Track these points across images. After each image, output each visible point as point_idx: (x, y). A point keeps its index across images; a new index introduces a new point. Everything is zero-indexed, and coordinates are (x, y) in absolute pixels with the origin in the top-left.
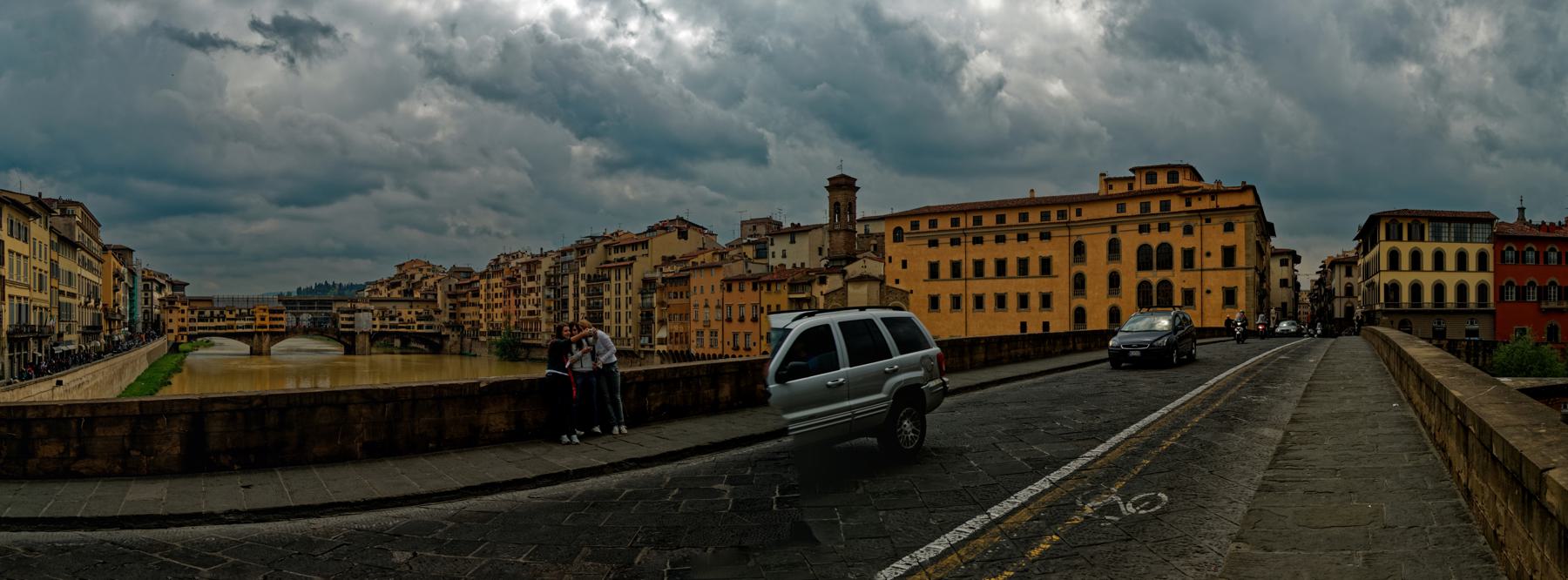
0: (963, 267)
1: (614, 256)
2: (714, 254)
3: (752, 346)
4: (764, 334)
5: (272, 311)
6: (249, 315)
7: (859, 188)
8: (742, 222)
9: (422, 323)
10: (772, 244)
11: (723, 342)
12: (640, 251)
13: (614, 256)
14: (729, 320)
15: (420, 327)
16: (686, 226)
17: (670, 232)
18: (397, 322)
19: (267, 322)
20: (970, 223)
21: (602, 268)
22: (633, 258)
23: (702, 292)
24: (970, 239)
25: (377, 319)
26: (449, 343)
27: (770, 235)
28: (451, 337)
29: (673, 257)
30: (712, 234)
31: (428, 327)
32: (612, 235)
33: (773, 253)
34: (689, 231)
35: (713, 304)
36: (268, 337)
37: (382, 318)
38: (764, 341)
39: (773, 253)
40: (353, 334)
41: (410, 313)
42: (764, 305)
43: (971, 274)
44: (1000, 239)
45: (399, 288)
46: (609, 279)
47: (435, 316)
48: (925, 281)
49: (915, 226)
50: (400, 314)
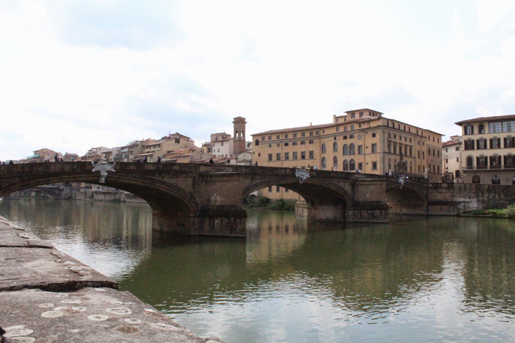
0: (281, 155)
1: (146, 150)
2: (190, 150)
7: (247, 122)
8: (211, 135)
10: (214, 146)
12: (157, 148)
13: (146, 150)
16: (179, 137)
17: (171, 140)
20: (284, 138)
22: (154, 152)
24: (284, 144)
26: (63, 193)
27: (213, 142)
28: (65, 190)
29: (172, 151)
30: (192, 141)
32: (146, 140)
33: (214, 150)
34: (181, 140)
39: (214, 150)
43: (284, 159)
44: (294, 144)
48: (267, 162)
49: (263, 139)
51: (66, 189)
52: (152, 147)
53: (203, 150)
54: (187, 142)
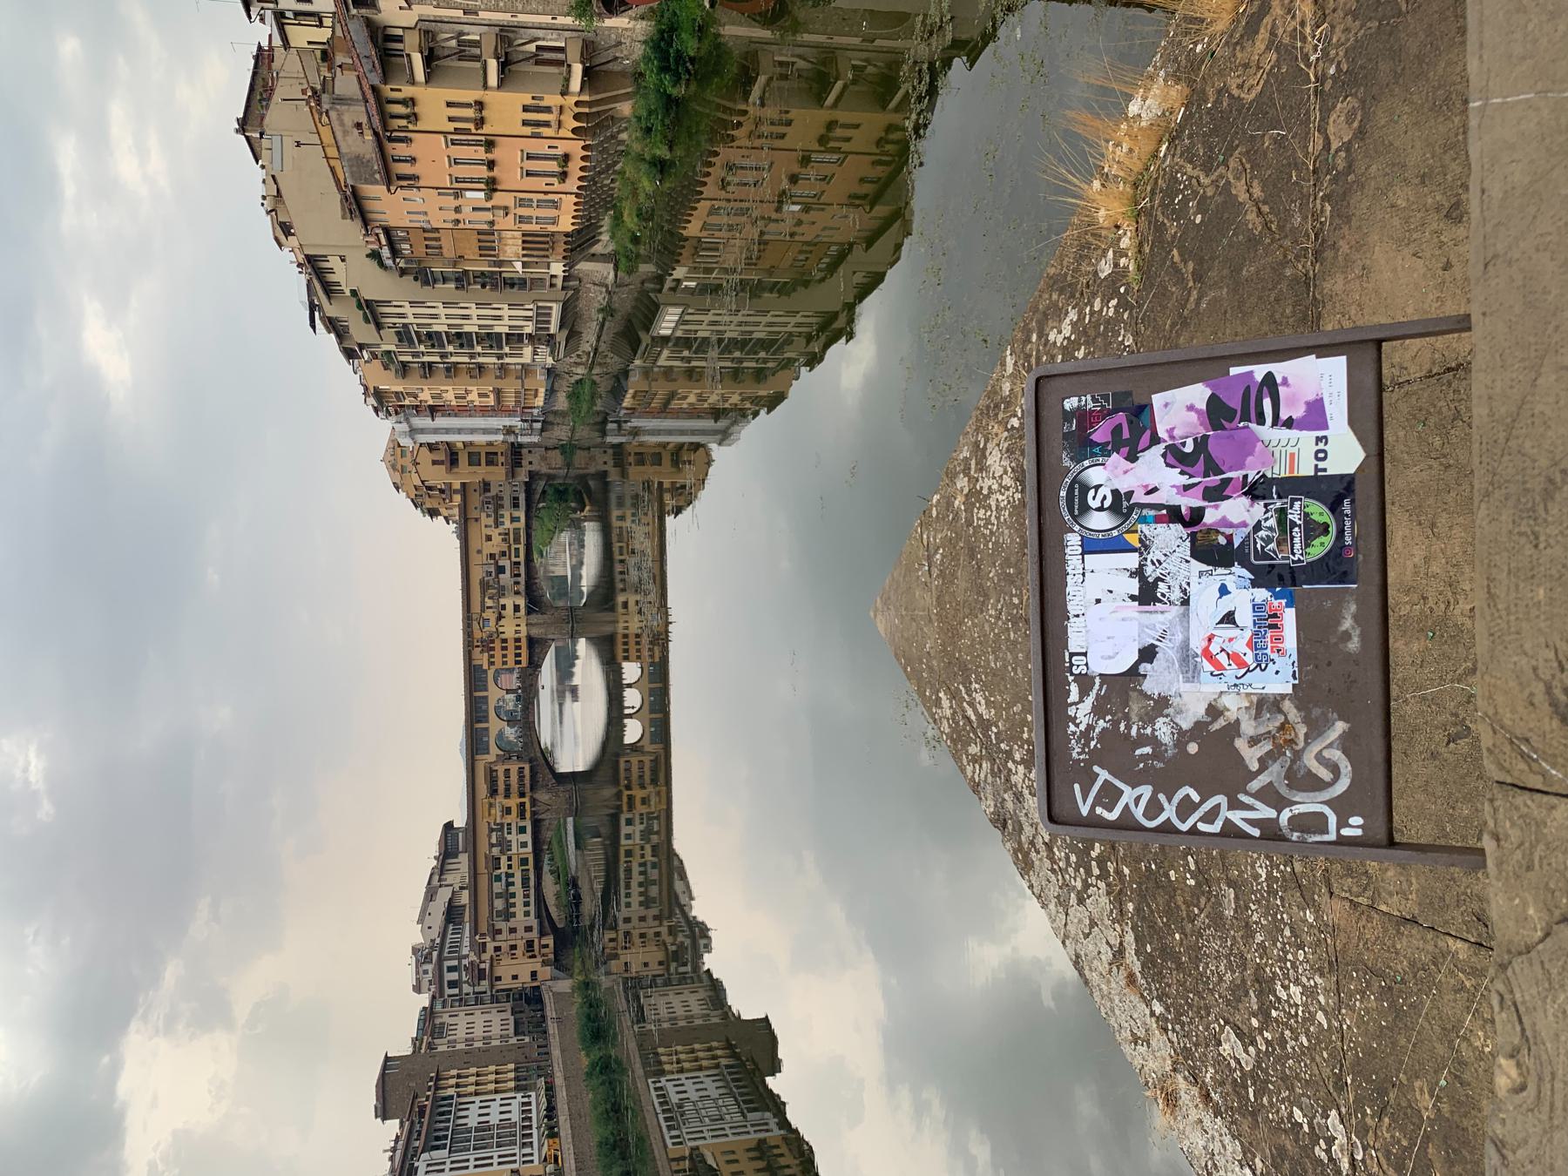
3: (559, 152)
4: (528, 130)
5: (493, 792)
6: (501, 830)
9: (507, 514)
11: (546, 193)
12: (334, 262)
14: (492, 186)
15: (514, 519)
18: (505, 562)
19: (513, 802)
21: (379, 326)
23: (426, 213)
25: (502, 601)
26: (544, 470)
28: (533, 468)
31: (516, 506)
35: (451, 202)
36: (543, 796)
37: (501, 592)
38: (545, 131)
40: (532, 642)
41: (489, 538)
42: (451, 127)
45: (442, 510)
46: (405, 326)
47: (494, 491)
50: (492, 556)
51: (530, 463)
52: (331, 278)
53: (309, 43)
54: (277, 98)
